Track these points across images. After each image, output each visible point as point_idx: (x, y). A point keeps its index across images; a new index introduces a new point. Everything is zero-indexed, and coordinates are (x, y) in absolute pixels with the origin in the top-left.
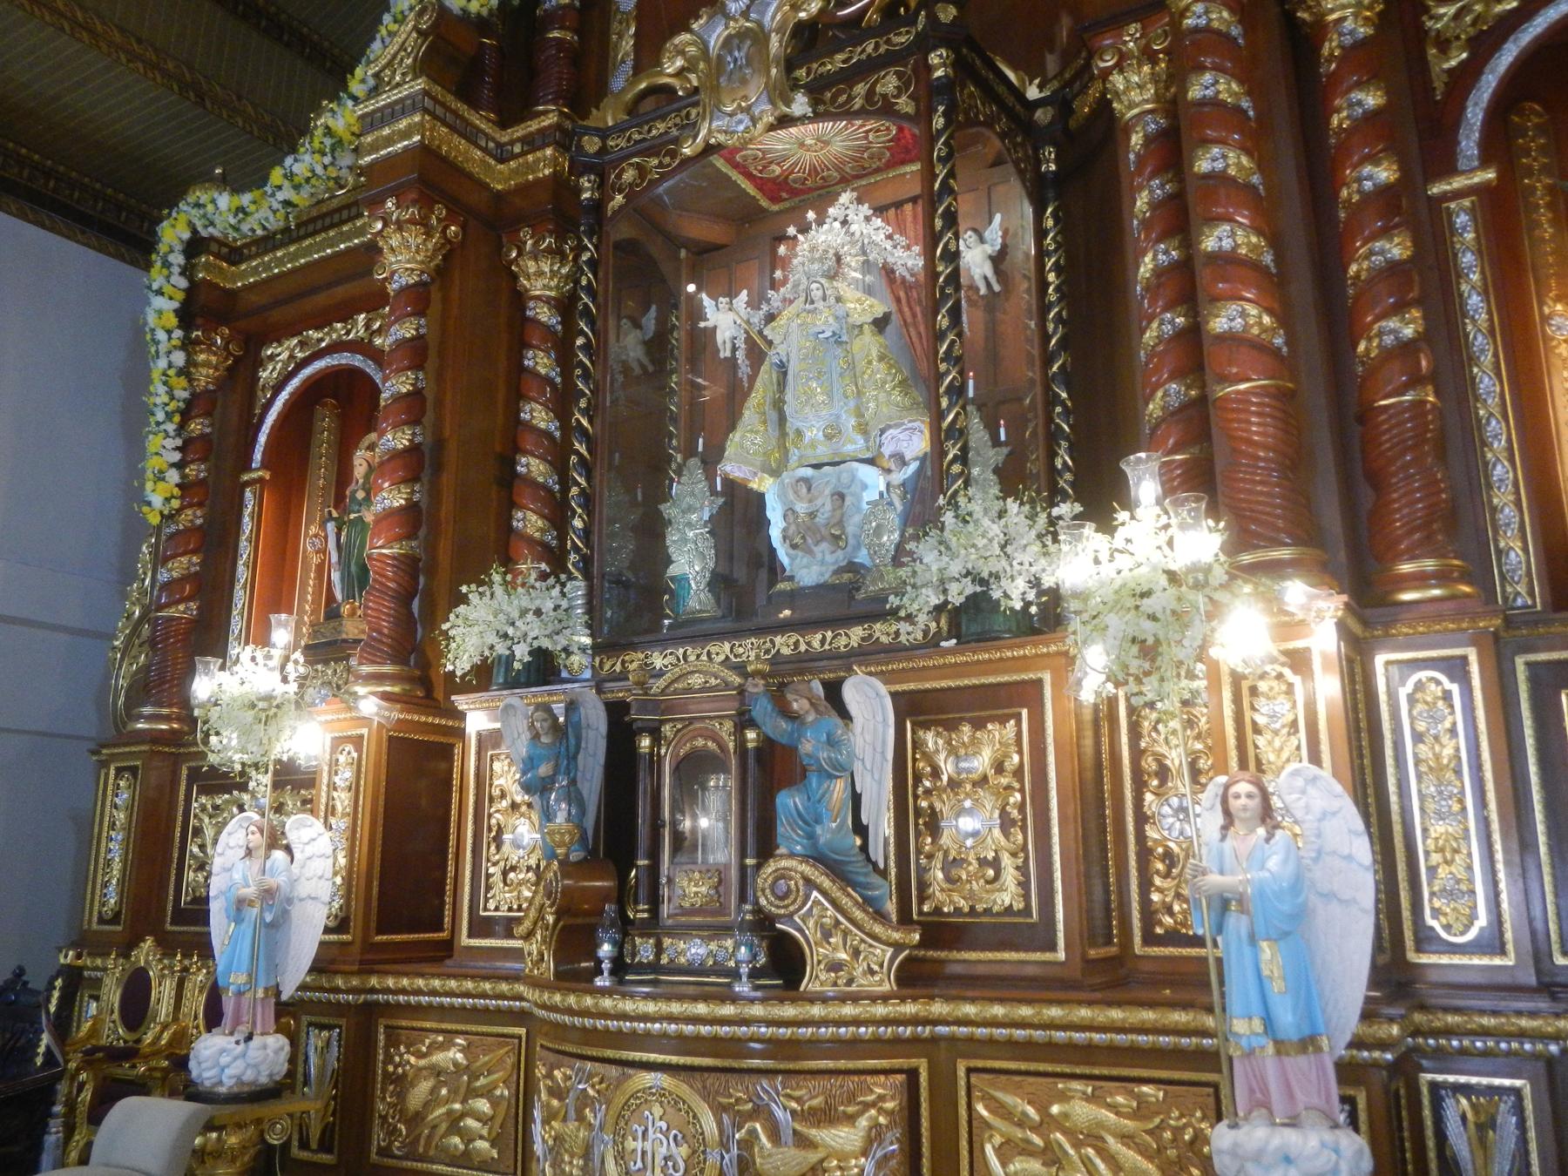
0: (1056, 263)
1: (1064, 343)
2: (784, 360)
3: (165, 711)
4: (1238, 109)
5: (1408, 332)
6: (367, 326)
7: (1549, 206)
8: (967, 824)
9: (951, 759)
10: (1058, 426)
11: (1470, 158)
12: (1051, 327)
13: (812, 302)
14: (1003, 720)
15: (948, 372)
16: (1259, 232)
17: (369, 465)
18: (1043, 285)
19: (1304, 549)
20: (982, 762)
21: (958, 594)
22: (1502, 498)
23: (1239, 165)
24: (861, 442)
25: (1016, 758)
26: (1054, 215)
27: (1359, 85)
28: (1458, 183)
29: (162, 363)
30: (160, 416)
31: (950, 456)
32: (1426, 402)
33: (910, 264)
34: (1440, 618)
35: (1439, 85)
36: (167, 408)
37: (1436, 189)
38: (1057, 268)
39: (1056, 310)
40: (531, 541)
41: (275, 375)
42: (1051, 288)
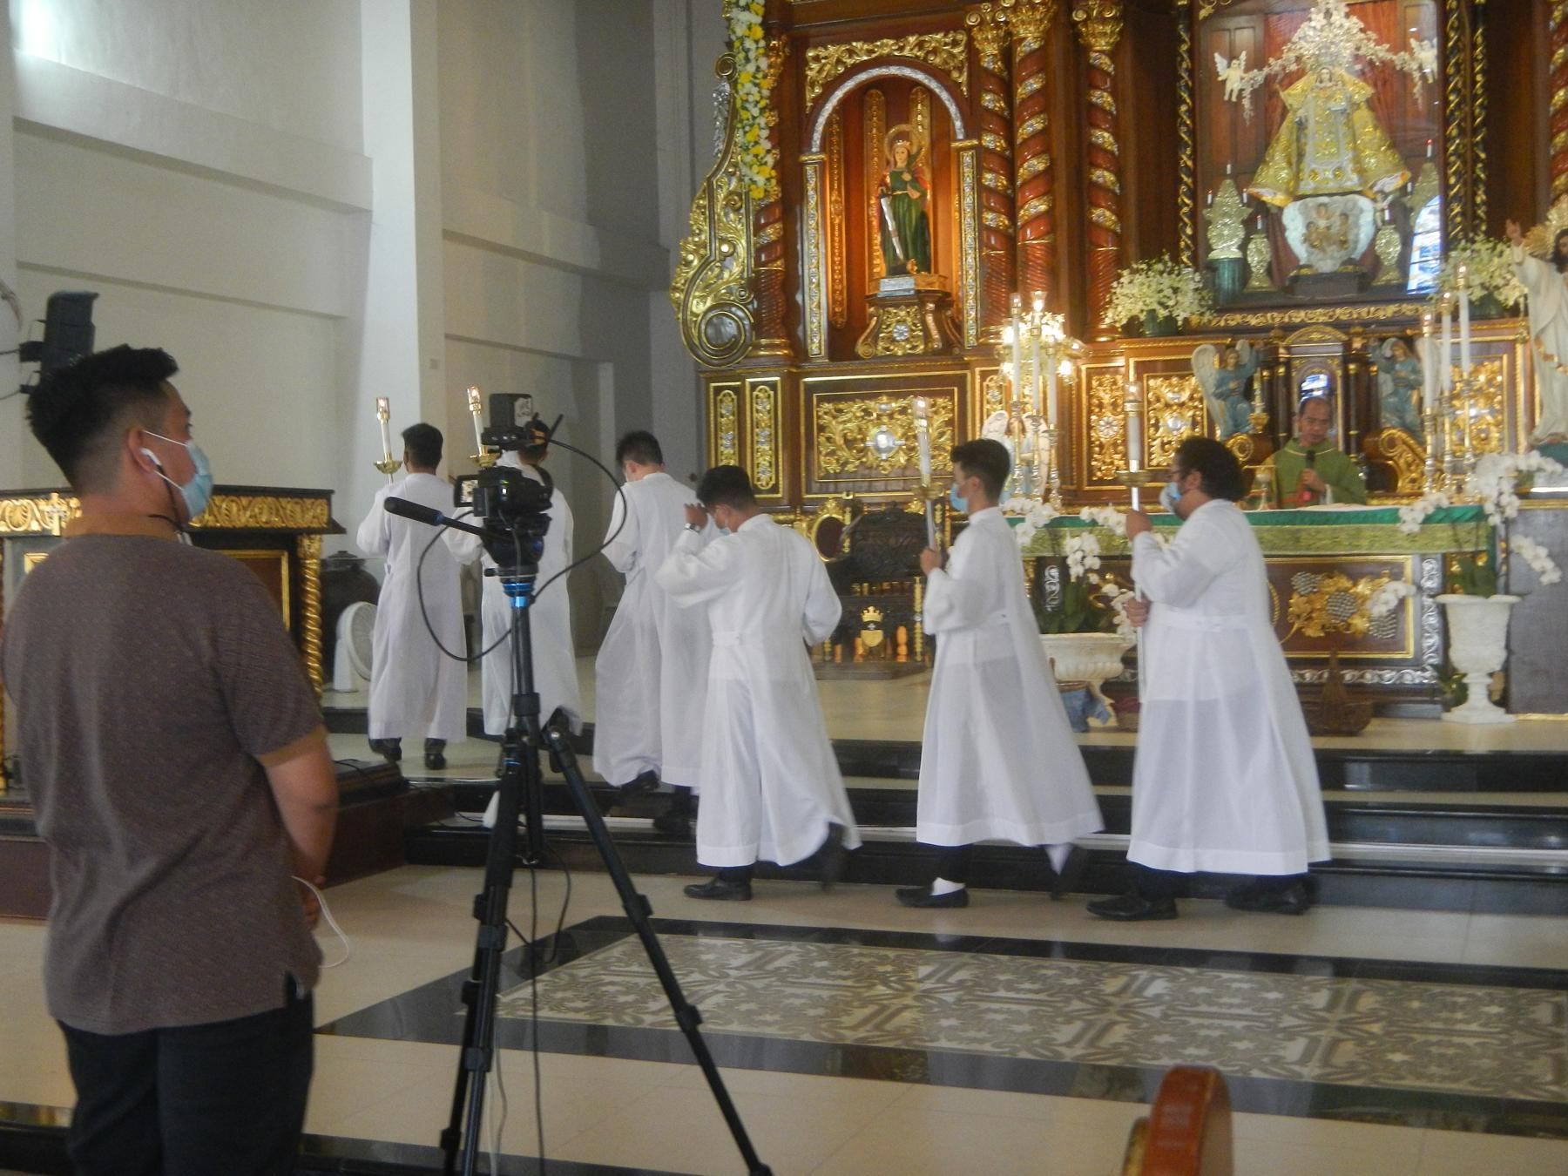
1: (1483, 123)
2: (1303, 120)
3: (777, 341)
6: (920, 45)
10: (1478, 176)
12: (1477, 111)
13: (1321, 82)
14: (1492, 360)
15: (1455, 163)
17: (909, 152)
18: (1474, 83)
21: (1478, 293)
24: (1355, 177)
26: (1482, 34)
29: (751, 68)
30: (756, 112)
33: (1381, 54)
36: (760, 105)
38: (1483, 71)
39: (1480, 100)
40: (1108, 230)
41: (825, 73)
42: (1478, 85)
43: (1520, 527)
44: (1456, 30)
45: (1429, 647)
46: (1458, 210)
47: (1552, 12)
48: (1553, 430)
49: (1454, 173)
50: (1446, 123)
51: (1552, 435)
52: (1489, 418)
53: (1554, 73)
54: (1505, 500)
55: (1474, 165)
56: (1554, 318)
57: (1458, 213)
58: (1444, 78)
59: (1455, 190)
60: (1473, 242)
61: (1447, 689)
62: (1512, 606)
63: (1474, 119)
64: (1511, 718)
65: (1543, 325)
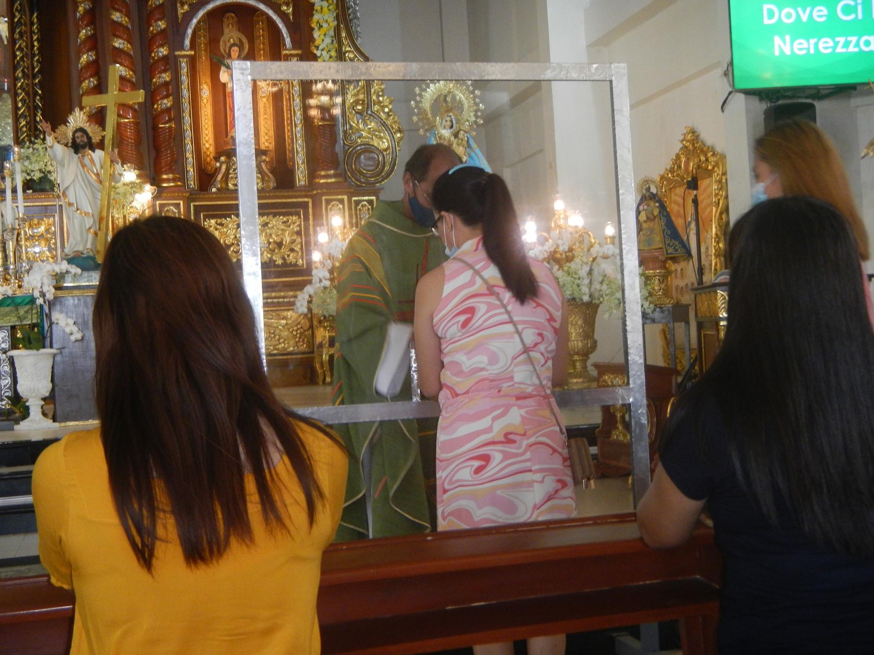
0: (38, 38)
4: (126, 28)
5: (169, 105)
7: (205, 51)
8: (37, 250)
9: (31, 229)
10: (38, 104)
11: (187, 46)
12: (36, 64)
14: (48, 217)
15: (21, 94)
16: (132, 71)
18: (33, 46)
19: (142, 172)
20: (42, 229)
21: (37, 176)
22: (189, 155)
23: (127, 47)
25: (53, 229)
26: (37, 17)
27: (160, 20)
28: (183, 53)
31: (22, 124)
32: (172, 127)
34: (174, 192)
35: (180, 16)
37: (177, 53)
39: (37, 57)
42: (35, 48)
43: (58, 307)
44: (19, 12)
45: (5, 386)
46: (24, 123)
47: (78, 7)
48: (76, 249)
49: (21, 100)
50: (15, 68)
51: (75, 252)
52: (48, 253)
53: (80, 44)
54: (45, 289)
55: (34, 97)
56: (74, 180)
57: (24, 125)
58: (12, 40)
59: (22, 111)
60: (34, 143)
61: (17, 410)
62: (54, 356)
63: (33, 68)
64: (57, 425)
65: (66, 186)
